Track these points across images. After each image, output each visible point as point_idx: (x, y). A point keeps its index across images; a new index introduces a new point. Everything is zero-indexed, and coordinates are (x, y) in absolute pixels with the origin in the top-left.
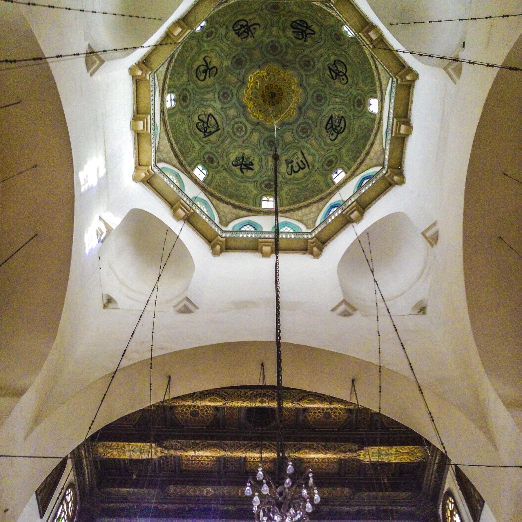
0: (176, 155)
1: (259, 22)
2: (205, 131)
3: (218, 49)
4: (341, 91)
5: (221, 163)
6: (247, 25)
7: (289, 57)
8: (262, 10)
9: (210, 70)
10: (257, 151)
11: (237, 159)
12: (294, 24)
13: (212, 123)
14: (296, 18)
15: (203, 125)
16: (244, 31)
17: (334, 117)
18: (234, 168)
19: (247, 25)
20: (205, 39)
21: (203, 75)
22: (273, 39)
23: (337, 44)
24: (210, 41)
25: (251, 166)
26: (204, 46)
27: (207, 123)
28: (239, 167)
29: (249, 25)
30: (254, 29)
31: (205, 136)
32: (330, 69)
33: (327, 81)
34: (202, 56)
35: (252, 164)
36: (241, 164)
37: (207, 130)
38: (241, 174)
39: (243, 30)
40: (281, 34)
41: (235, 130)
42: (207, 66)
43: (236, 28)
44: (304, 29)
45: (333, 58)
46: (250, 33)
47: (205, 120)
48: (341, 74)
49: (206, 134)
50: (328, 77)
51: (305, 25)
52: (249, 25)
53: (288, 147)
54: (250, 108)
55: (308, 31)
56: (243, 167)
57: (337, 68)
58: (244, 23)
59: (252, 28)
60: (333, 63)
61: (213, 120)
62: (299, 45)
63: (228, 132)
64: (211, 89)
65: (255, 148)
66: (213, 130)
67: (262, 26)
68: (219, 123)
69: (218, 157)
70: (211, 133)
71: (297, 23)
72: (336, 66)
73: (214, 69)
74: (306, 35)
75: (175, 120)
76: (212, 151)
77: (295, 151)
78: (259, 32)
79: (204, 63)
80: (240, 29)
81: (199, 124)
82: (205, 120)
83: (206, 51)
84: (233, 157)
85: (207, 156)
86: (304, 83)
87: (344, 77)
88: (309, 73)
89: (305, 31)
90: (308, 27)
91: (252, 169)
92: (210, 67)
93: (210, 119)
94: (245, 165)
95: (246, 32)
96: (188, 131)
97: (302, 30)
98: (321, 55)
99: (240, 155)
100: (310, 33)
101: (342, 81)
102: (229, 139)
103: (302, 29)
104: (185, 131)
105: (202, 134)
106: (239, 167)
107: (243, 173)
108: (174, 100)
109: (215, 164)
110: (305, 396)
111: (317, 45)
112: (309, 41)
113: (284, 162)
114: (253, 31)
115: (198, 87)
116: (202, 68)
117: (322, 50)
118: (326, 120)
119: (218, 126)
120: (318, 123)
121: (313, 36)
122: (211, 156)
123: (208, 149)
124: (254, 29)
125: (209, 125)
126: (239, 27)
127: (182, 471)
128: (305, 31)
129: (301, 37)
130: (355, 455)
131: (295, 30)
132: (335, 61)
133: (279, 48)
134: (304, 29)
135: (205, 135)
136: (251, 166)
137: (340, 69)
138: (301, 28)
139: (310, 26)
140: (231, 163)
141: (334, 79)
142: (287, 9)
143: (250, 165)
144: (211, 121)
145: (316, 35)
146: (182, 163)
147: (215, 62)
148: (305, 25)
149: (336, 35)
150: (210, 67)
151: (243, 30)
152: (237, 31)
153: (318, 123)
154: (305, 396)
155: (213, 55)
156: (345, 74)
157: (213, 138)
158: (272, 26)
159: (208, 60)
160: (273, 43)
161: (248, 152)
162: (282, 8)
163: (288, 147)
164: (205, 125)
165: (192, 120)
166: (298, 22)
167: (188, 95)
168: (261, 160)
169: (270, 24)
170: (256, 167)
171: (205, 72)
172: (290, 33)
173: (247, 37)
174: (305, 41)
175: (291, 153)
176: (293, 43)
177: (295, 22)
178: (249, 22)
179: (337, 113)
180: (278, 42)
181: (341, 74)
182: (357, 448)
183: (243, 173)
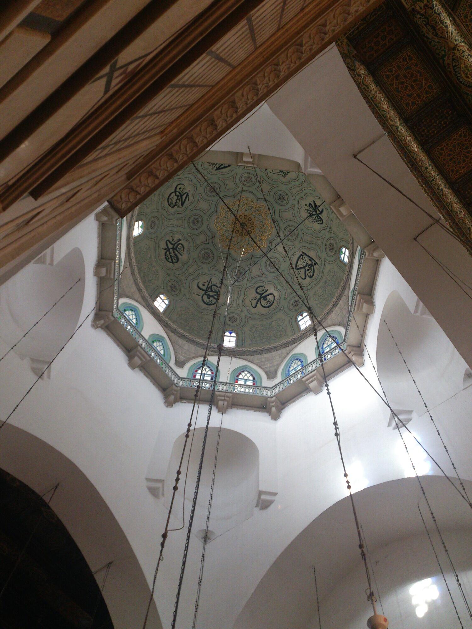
0: (335, 305)
1: (196, 287)
2: (311, 265)
3: (240, 301)
4: (191, 181)
5: (328, 236)
6: (205, 294)
7: (202, 238)
8: (185, 295)
9: (261, 294)
10: (297, 206)
11: (315, 221)
12: (174, 261)
13: (302, 263)
14: (170, 265)
15: (308, 270)
16: (212, 291)
17: (215, 168)
18: (324, 221)
19: (205, 294)
20: (238, 320)
21: (268, 297)
22: (199, 263)
23: (158, 219)
24: (238, 314)
25: (313, 205)
26: (246, 316)
27: (304, 267)
28: (320, 215)
29: (203, 292)
30: (204, 285)
31: (316, 263)
32: (182, 204)
33: (194, 196)
34: (253, 310)
35: (310, 204)
36: (318, 215)
37: (310, 264)
38: (324, 210)
39: (211, 294)
40: (191, 261)
41: (294, 237)
42: (259, 299)
43: (214, 300)
44: (171, 250)
45: (172, 210)
46: (210, 285)
47: (303, 270)
48: (178, 194)
49: (314, 263)
50: (191, 198)
51: (168, 253)
52: (203, 292)
53: (274, 183)
54: (268, 236)
55: (170, 246)
56: (318, 212)
57: (176, 200)
58: (205, 297)
59: (205, 288)
60: (176, 207)
61: (299, 263)
62: (187, 240)
63: (300, 242)
64: (276, 281)
65: (296, 209)
66: (307, 258)
67: (197, 282)
68: (298, 256)
69: (325, 240)
70: (311, 259)
71: (172, 260)
72: (176, 203)
73: (259, 291)
74: (175, 244)
75: (317, 305)
76: (324, 250)
77: (270, 174)
78: (203, 279)
79: (259, 303)
80: (212, 296)
81: (309, 275)
82: (303, 270)
83: (248, 311)
84: (317, 226)
85: (330, 253)
86: (213, 209)
87: (178, 190)
88: (202, 213)
89: (173, 249)
90: (168, 249)
91: (314, 202)
92: (259, 296)
93: (300, 266)
94: (316, 212)
95: (211, 289)
96: (321, 284)
97: (174, 252)
98: (178, 219)
99: (311, 219)
100: (171, 244)
101: (182, 188)
102: (305, 237)
103: (172, 252)
104: (321, 288)
105: (316, 267)
106: (320, 215)
107: (322, 210)
108: (302, 315)
109: (332, 242)
110: (466, 85)
111: (175, 229)
112: (177, 237)
113: (287, 177)
114: (206, 284)
115: (280, 296)
116: (264, 303)
117: (175, 223)
118: (222, 170)
119: (301, 255)
120: (233, 173)
121: (171, 240)
122: (328, 249)
123: (323, 255)
124: (204, 285)
125: (305, 265)
126: (211, 299)
128: (173, 249)
129: (180, 245)
131: (178, 255)
132: (173, 207)
133: (203, 252)
134: (171, 250)
135: (315, 264)
136: (313, 205)
137: (175, 197)
138: (172, 253)
139: (166, 249)
140: (321, 225)
141: (188, 194)
142: (168, 278)
143: (312, 206)
144: (301, 264)
145: (168, 238)
146: (339, 296)
147: (253, 294)
148: (168, 253)
149: (152, 227)
150: (259, 296)
151: (211, 294)
152: (216, 297)
153: (233, 173)
154: (466, 85)
155: (247, 301)
156: (175, 192)
157: (312, 254)
158: (191, 274)
159: (254, 303)
160: (204, 261)
161: (304, 214)
162: (170, 284)
163: (274, 183)
164: (307, 268)
165: (310, 283)
166: (170, 260)
167: (292, 302)
168: (301, 199)
169: (191, 277)
170: (310, 200)
171: (265, 298)
172: (184, 257)
173: (215, 285)
174: (180, 240)
175: (275, 177)
176: (190, 246)
177: (173, 262)
178: (201, 295)
179: (211, 168)
180: (199, 257)
181: (178, 194)
183: (322, 210)
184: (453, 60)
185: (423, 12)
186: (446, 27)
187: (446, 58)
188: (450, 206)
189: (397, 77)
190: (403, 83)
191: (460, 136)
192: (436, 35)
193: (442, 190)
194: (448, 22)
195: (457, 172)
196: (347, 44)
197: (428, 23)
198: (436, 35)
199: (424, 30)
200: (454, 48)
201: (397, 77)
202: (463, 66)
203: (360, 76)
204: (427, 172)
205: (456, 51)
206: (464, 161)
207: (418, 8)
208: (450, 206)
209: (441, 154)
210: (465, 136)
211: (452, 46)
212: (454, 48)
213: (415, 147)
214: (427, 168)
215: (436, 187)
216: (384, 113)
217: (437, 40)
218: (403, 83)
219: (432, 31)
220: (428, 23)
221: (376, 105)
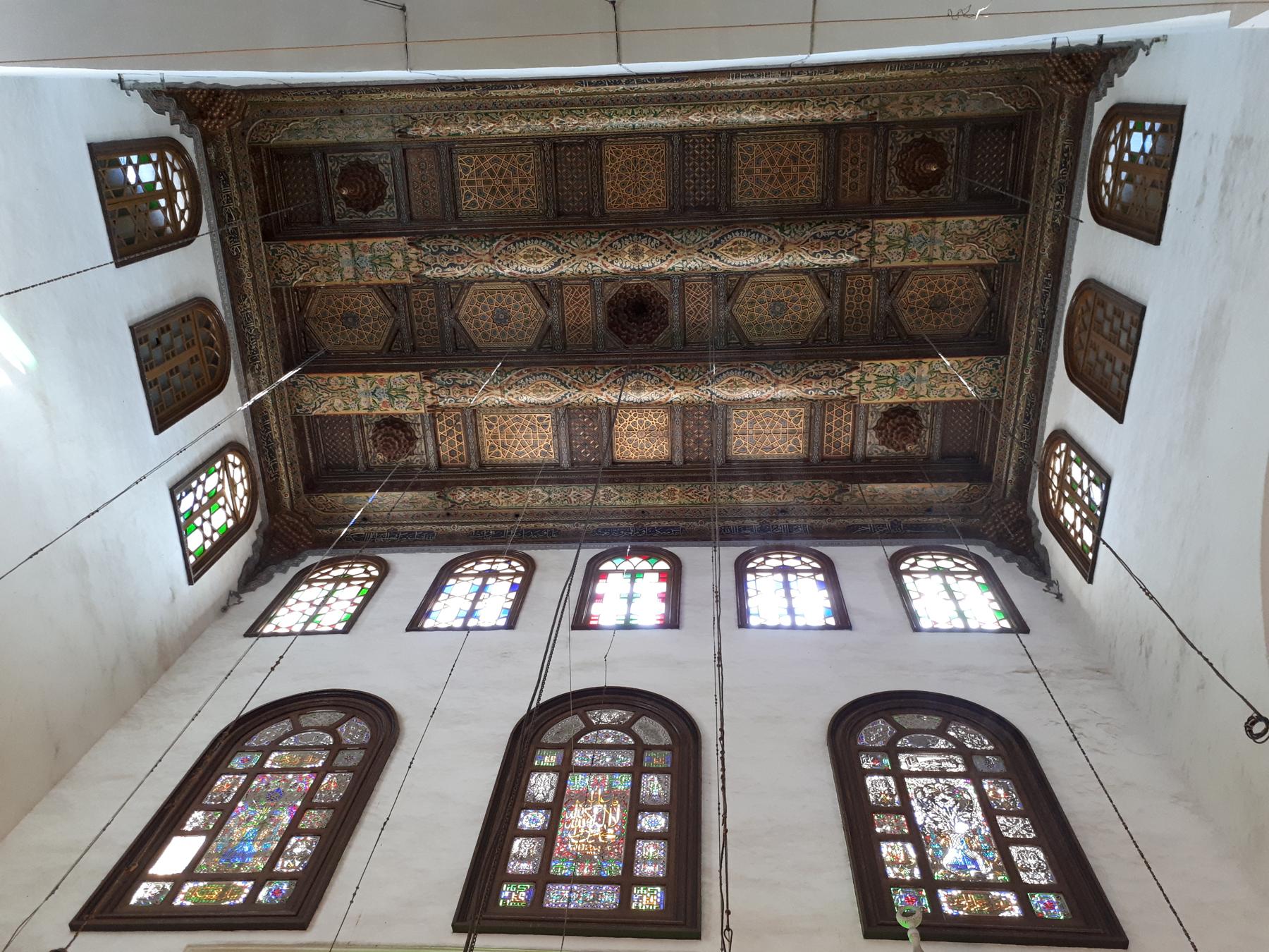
127: (481, 465)
130: (839, 383)
182: (844, 369)
184: (770, 239)
185: (854, 238)
186: (814, 255)
187: (778, 231)
188: (579, 113)
189: (794, 159)
190: (781, 162)
191: (658, 194)
192: (815, 237)
193: (610, 117)
194: (817, 261)
195: (613, 158)
196: (896, 116)
197: (836, 235)
198: (815, 237)
199: (831, 226)
200: (782, 248)
201: (794, 159)
202: (754, 246)
203: (845, 106)
204: (650, 112)
205: (777, 248)
206: (620, 177)
207: (864, 233)
208: (579, 113)
209: (651, 152)
210: (653, 199)
211: (786, 248)
212: (782, 248)
213: (695, 119)
214: (656, 115)
215: (620, 112)
216: (774, 105)
217: (808, 233)
218: (781, 162)
219: (823, 234)
220: (836, 235)
221: (792, 102)
